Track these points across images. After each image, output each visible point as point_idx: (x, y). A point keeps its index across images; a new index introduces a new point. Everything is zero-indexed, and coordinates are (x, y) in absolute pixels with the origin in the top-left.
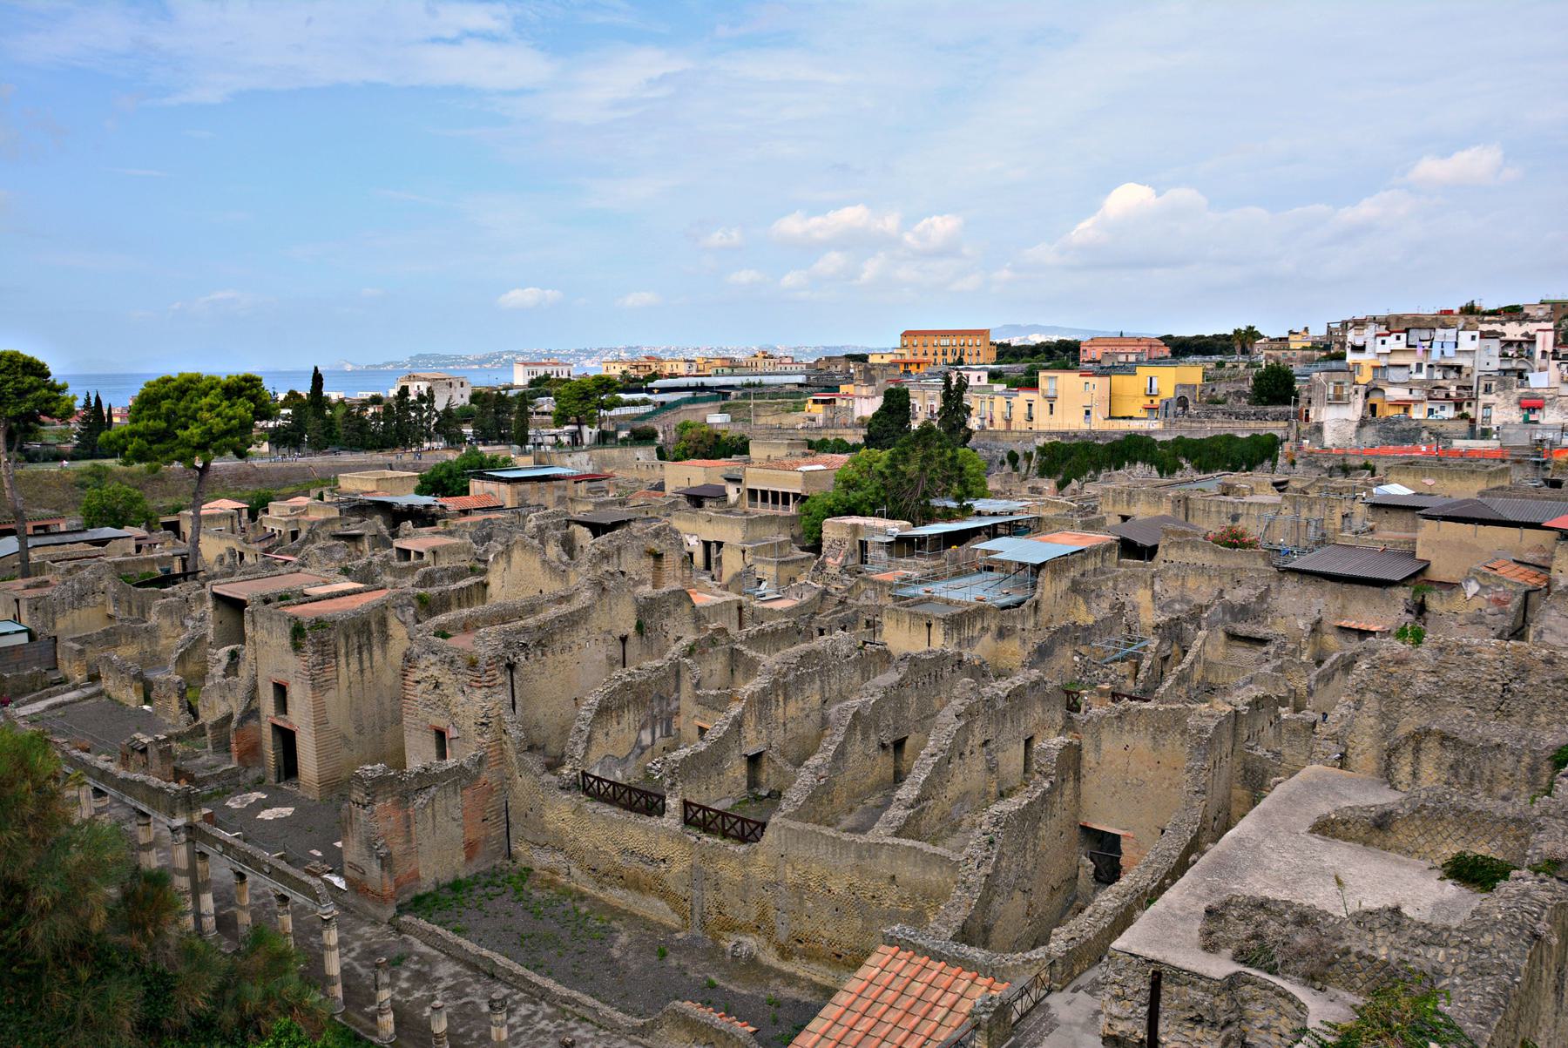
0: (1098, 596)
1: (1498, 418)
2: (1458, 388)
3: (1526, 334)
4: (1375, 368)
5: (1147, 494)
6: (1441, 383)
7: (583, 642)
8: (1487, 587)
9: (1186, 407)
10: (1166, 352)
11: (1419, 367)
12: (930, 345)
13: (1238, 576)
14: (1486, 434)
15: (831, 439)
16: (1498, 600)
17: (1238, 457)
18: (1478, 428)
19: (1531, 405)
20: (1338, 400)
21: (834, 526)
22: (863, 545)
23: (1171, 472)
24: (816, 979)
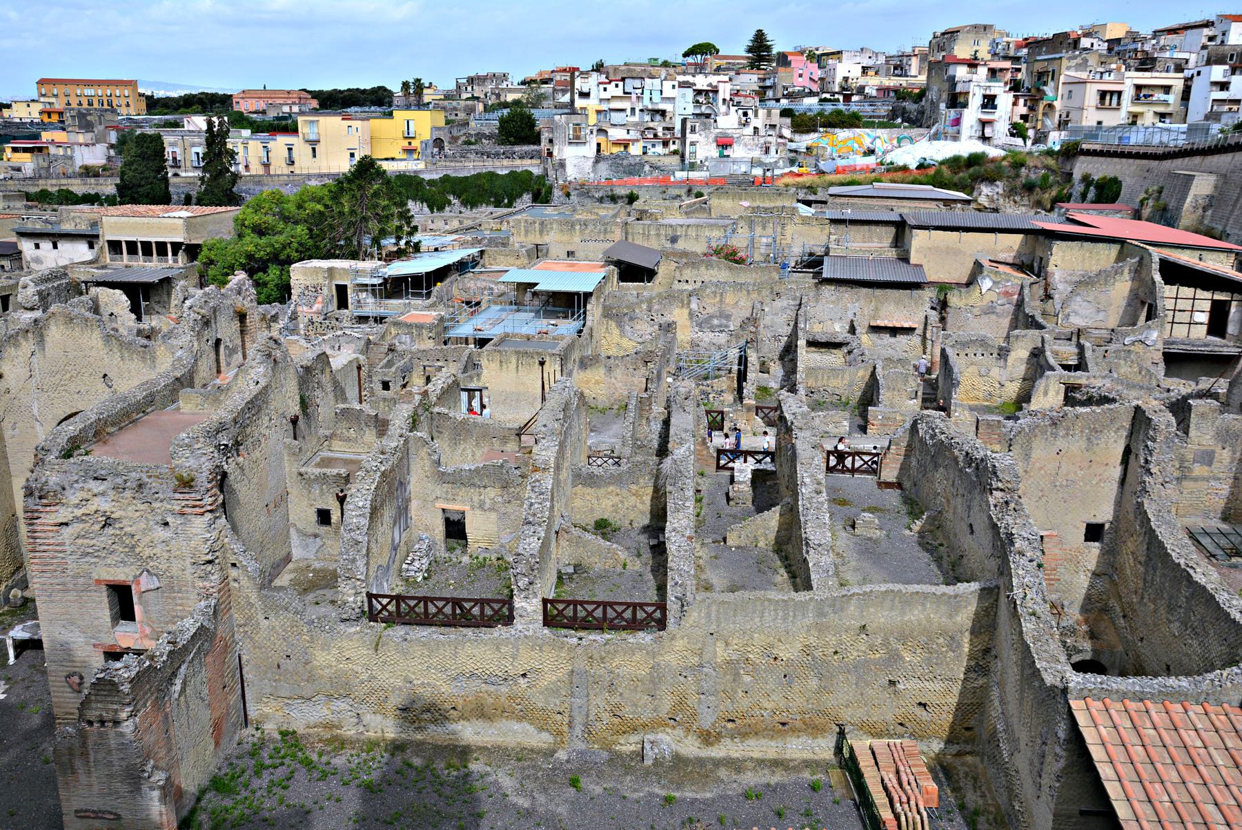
0: (631, 319)
1: (700, 156)
2: (664, 129)
3: (710, 85)
4: (599, 112)
5: (560, 223)
6: (651, 125)
7: (267, 432)
8: (999, 282)
9: (441, 148)
10: (315, 104)
11: (633, 110)
12: (73, 95)
13: (776, 289)
14: (692, 167)
15: (54, 190)
16: (1007, 292)
17: (500, 191)
18: (687, 162)
19: (724, 144)
20: (577, 140)
21: (306, 272)
22: (342, 291)
23: (441, 209)
24: (756, 755)
